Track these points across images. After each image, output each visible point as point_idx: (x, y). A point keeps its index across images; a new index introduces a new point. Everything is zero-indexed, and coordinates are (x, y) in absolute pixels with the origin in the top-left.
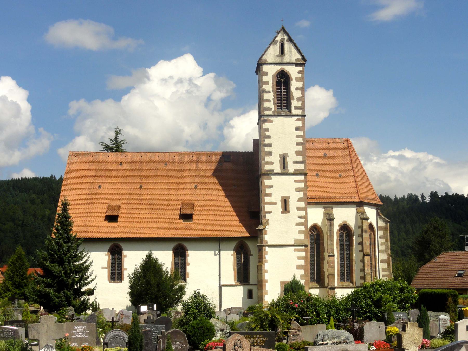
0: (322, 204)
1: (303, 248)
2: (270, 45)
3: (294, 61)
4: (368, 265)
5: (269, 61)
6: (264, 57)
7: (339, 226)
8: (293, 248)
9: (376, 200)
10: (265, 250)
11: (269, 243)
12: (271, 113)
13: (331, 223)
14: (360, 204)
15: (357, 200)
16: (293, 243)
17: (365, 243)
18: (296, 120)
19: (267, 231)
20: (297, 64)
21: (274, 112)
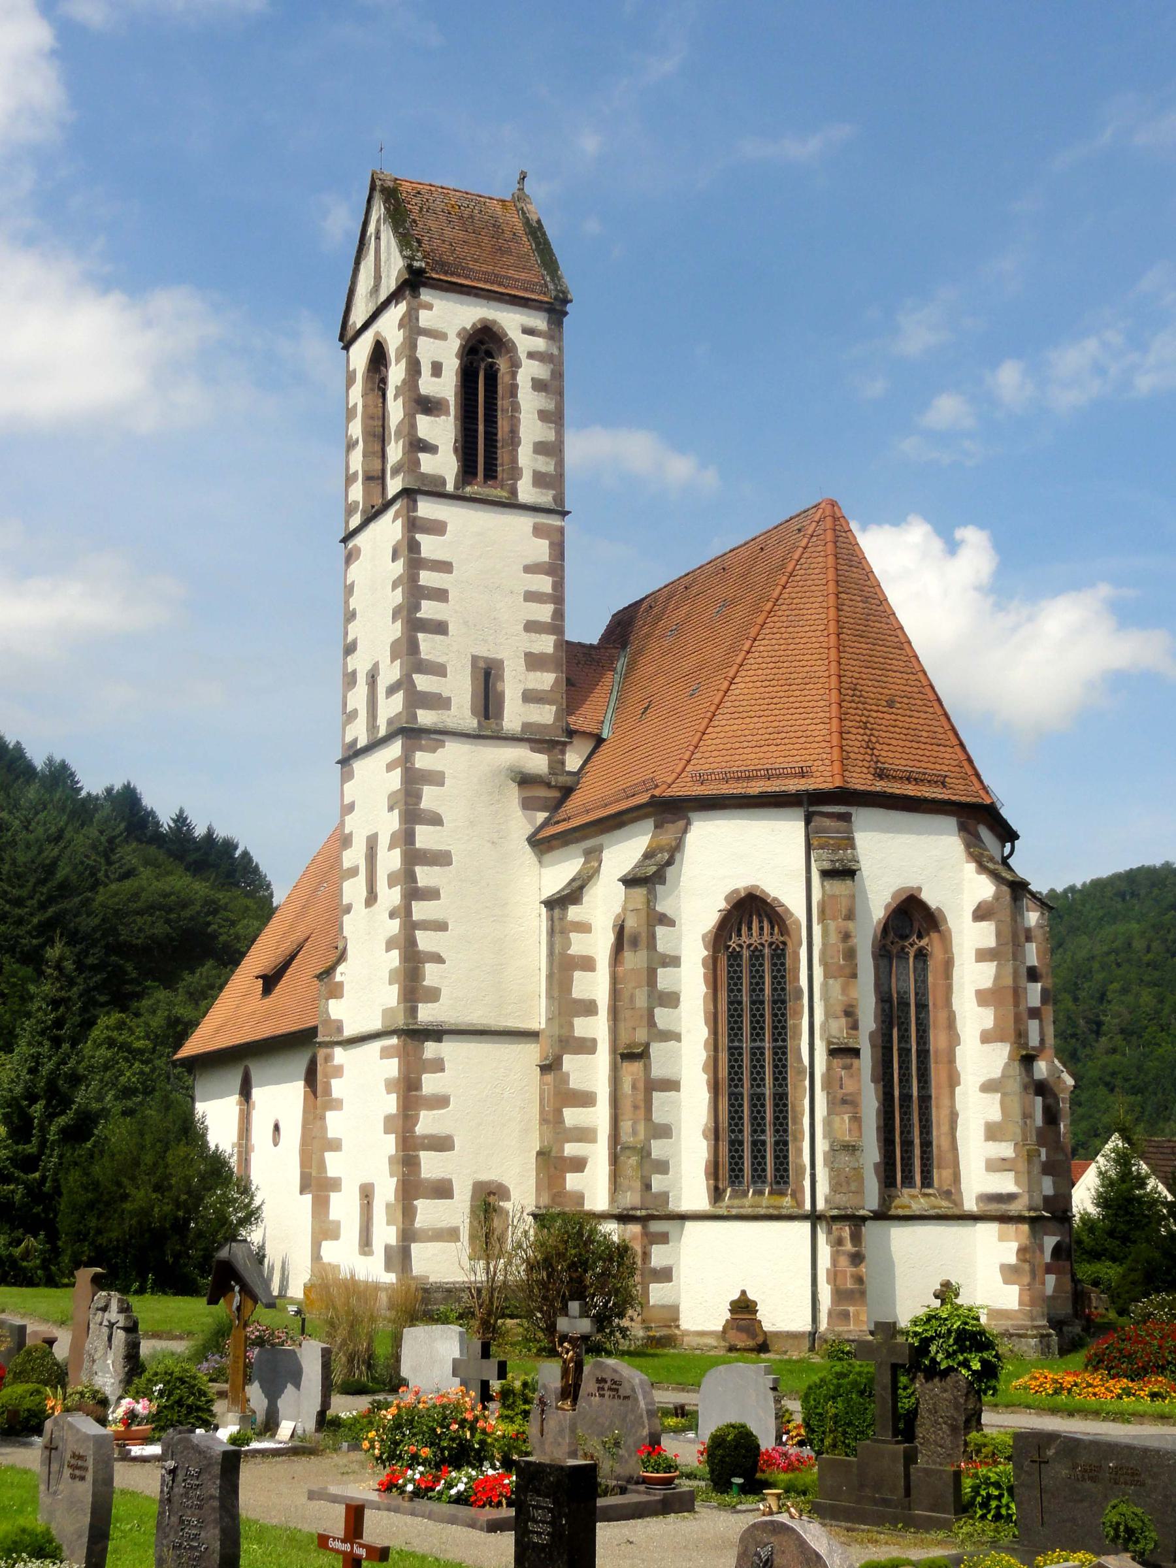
0: (578, 840)
1: (394, 1041)
2: (357, 263)
3: (393, 287)
4: (636, 1107)
5: (359, 326)
6: (351, 322)
7: (614, 926)
8: (376, 1046)
9: (802, 774)
10: (328, 1058)
11: (349, 1032)
12: (355, 521)
13: (551, 919)
14: (672, 810)
15: (644, 798)
16: (376, 1025)
17: (632, 998)
18: (393, 521)
19: (341, 984)
20: (394, 297)
21: (364, 512)
